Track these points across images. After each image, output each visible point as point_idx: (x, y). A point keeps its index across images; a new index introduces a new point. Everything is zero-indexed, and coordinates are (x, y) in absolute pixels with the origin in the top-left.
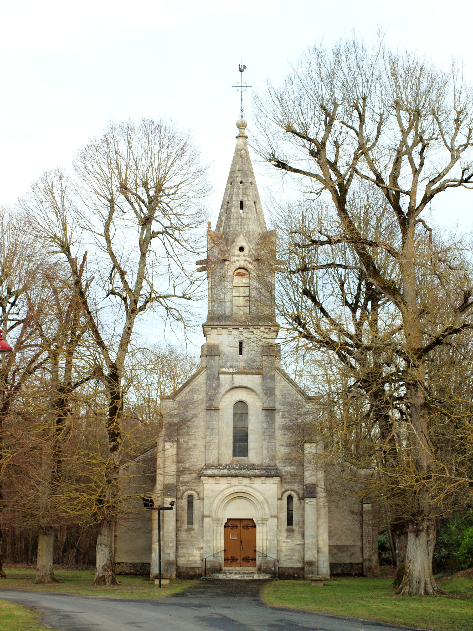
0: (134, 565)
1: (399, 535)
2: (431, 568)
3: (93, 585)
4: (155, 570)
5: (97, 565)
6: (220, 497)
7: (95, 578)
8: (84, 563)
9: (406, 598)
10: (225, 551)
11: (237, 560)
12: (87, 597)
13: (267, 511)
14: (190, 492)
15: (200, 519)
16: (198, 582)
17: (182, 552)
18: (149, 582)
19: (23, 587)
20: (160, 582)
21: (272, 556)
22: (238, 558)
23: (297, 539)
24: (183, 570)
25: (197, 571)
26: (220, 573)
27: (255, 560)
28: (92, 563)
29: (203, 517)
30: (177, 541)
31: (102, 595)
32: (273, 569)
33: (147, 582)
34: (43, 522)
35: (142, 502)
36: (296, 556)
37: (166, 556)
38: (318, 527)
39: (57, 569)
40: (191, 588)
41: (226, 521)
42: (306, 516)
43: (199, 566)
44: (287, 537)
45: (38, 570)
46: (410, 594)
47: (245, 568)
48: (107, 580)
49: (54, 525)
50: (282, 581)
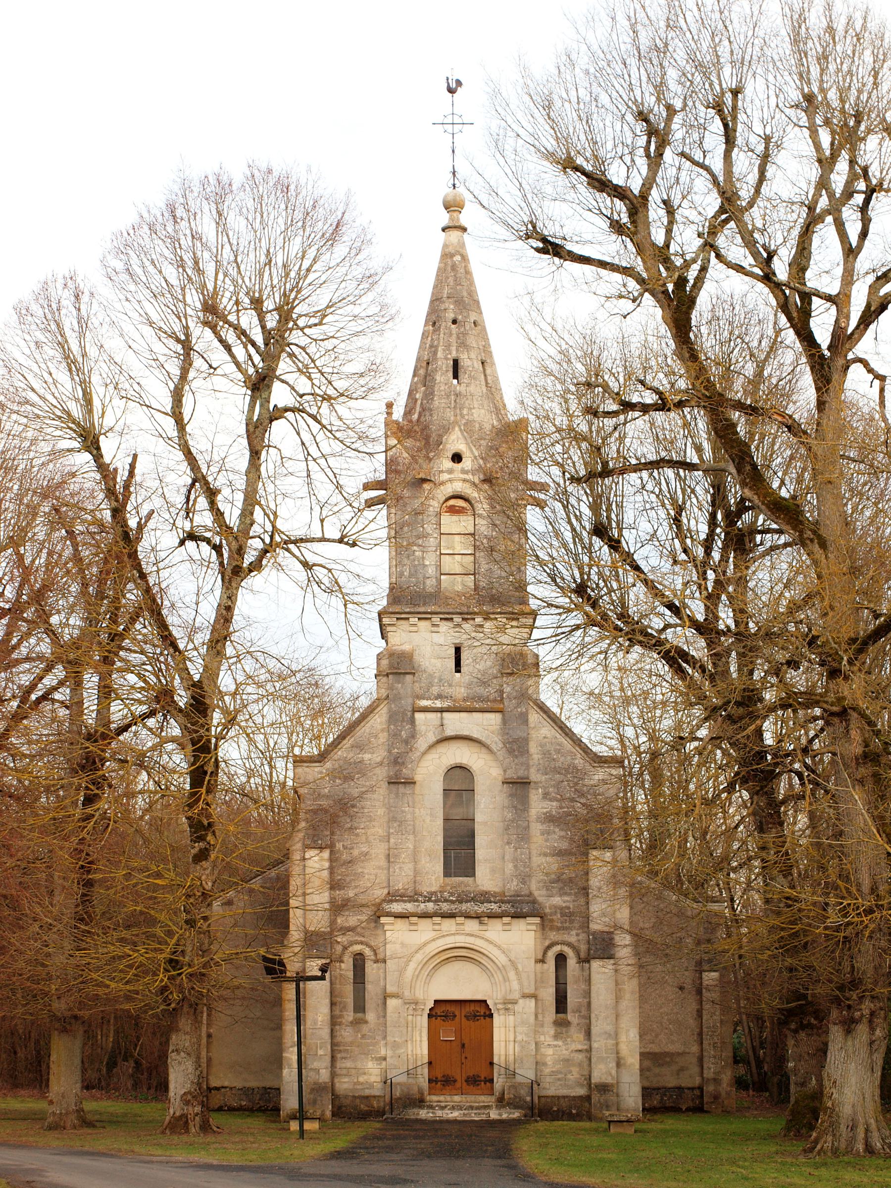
0: (246, 1091)
1: (796, 1031)
2: (877, 1098)
3: (163, 1133)
4: (290, 1102)
5: (171, 1094)
6: (419, 957)
7: (168, 1118)
8: (149, 1088)
9: (829, 1160)
10: (430, 1063)
11: (455, 1081)
12: (148, 1158)
13: (515, 985)
14: (357, 948)
15: (380, 1002)
16: (378, 1125)
17: (344, 1065)
18: (279, 1126)
19: (20, 1136)
20: (301, 1126)
21: (526, 1073)
22: (458, 1078)
23: (577, 1040)
24: (347, 1102)
25: (375, 1104)
26: (421, 1107)
27: (492, 1081)
28: (164, 1086)
29: (385, 997)
30: (333, 1044)
31: (180, 1156)
32: (528, 1099)
33: (273, 1125)
34: (60, 1006)
35: (261, 965)
36: (575, 1074)
37: (312, 1074)
38: (617, 1016)
39: (94, 1098)
40: (365, 1138)
41: (431, 1004)
42: (593, 995)
43: (377, 1094)
44: (556, 1037)
45: (51, 1102)
46: (835, 1152)
47: (471, 1098)
48: (191, 1124)
49: (81, 1013)
50: (547, 1123)
